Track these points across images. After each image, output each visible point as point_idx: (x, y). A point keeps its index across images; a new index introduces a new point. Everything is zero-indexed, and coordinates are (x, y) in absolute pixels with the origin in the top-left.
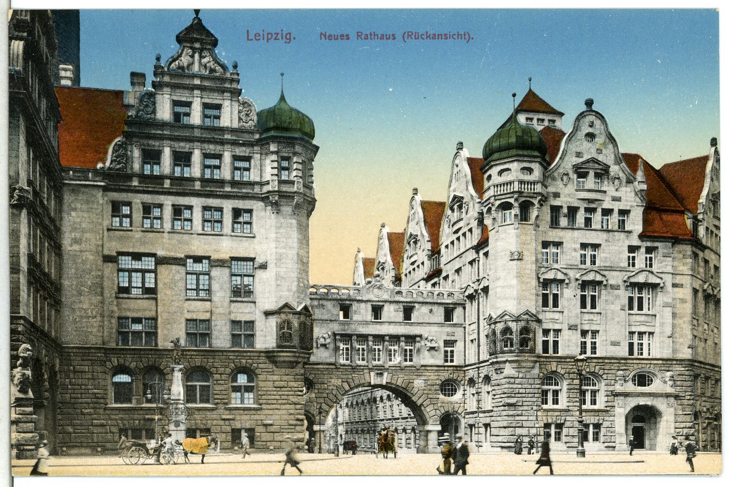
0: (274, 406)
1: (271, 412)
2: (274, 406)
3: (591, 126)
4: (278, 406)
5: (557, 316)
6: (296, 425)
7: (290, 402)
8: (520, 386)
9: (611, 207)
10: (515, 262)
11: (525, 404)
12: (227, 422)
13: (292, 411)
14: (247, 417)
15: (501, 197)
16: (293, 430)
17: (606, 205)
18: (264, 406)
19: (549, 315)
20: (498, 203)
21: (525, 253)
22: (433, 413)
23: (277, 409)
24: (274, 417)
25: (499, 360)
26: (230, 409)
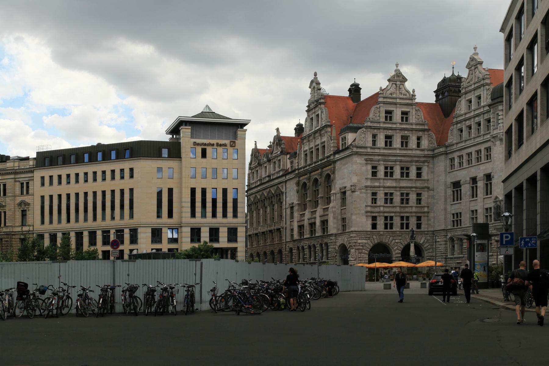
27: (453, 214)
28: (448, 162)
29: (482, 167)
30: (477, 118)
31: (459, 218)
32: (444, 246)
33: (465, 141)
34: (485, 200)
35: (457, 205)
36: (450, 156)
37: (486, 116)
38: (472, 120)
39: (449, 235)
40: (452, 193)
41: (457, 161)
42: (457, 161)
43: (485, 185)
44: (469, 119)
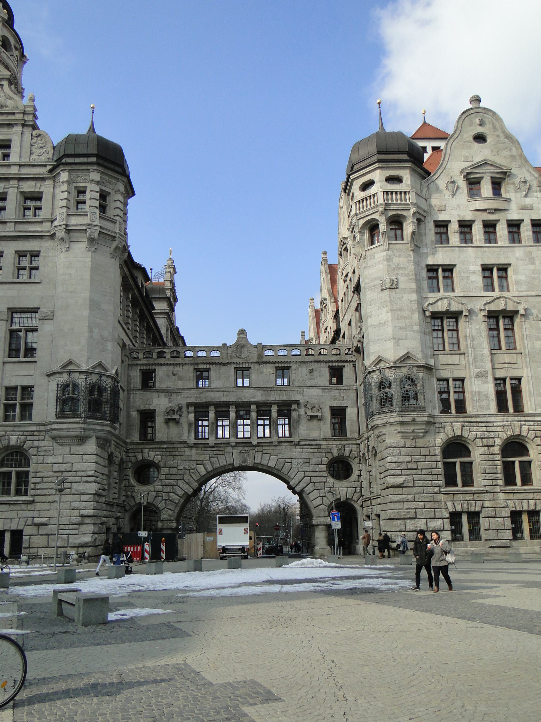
2: (51, 498)
3: (481, 125)
5: (455, 359)
7: (73, 492)
8: (408, 459)
9: (521, 218)
10: (387, 292)
11: (417, 484)
13: (76, 505)
14: (14, 514)
15: (362, 215)
16: (76, 531)
17: (514, 216)
18: (37, 499)
20: (362, 222)
21: (401, 280)
22: (318, 501)
24: (50, 513)
25: (376, 422)
34: (8, 367)
37: (28, 187)
43: (8, 333)
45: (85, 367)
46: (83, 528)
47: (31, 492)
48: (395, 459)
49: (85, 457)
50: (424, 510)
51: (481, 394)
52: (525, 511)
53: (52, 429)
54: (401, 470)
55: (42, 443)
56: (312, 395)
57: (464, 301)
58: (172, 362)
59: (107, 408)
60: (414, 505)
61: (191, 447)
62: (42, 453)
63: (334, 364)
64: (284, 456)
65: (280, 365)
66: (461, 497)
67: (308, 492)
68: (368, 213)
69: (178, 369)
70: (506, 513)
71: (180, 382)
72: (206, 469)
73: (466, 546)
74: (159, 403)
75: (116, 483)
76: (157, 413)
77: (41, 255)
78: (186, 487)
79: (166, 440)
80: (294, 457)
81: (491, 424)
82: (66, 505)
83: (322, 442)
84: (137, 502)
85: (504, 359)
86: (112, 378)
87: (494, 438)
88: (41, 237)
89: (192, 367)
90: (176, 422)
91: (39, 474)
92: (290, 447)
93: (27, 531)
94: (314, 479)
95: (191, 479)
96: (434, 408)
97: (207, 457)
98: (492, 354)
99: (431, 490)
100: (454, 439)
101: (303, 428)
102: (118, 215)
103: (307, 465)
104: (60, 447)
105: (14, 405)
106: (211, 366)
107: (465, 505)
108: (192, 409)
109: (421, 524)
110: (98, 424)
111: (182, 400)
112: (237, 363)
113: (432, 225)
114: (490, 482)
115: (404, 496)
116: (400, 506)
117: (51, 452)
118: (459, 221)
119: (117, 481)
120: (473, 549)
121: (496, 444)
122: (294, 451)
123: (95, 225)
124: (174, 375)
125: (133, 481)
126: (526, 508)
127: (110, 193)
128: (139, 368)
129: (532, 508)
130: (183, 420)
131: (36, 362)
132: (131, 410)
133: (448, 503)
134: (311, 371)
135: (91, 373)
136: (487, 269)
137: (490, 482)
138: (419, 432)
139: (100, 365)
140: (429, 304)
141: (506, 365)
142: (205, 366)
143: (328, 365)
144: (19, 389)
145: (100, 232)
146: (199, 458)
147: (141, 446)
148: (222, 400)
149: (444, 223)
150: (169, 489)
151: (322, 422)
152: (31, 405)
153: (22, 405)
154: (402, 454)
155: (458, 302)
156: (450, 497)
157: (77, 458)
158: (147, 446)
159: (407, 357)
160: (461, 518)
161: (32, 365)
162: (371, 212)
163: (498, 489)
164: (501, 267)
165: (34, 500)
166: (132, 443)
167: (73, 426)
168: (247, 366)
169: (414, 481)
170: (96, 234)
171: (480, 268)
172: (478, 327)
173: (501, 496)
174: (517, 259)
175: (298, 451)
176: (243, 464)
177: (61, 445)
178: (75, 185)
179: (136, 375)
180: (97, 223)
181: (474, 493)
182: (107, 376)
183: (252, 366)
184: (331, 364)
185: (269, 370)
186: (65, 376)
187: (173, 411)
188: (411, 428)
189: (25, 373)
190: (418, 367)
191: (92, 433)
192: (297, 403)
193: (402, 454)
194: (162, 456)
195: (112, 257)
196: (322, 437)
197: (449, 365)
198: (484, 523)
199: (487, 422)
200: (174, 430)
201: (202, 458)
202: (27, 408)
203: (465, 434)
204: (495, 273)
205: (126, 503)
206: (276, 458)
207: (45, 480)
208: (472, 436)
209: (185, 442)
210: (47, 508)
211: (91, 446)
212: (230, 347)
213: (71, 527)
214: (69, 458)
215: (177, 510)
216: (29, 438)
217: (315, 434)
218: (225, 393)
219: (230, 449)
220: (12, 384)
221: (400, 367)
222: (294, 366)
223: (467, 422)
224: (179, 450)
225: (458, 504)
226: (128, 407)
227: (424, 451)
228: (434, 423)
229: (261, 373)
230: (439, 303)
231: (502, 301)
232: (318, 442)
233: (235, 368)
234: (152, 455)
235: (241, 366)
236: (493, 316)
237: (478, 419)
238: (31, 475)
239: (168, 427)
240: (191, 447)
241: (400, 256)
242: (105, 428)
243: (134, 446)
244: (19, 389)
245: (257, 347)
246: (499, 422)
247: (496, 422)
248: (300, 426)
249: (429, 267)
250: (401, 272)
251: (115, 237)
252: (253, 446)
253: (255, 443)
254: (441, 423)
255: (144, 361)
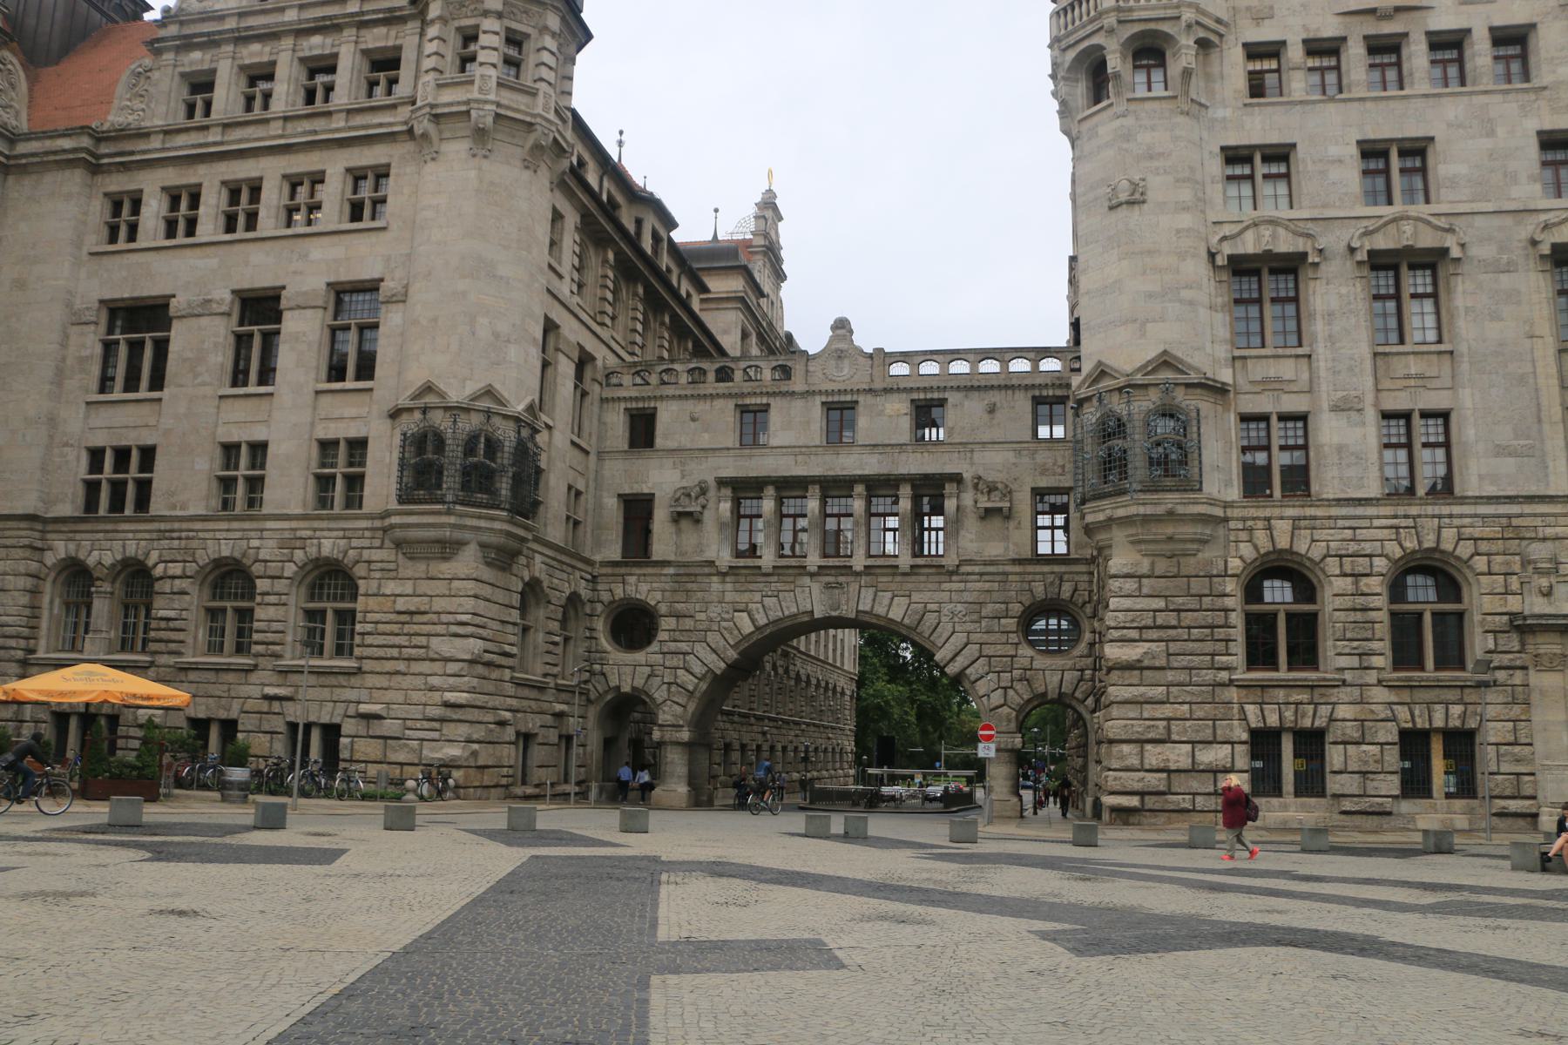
0: (389, 666)
1: (381, 681)
2: (389, 666)
4: (401, 666)
5: (1286, 369)
6: (442, 720)
7: (432, 655)
8: (1161, 604)
12: (276, 706)
13: (435, 681)
14: (325, 693)
16: (435, 735)
18: (368, 665)
19: (1258, 370)
22: (997, 698)
23: (398, 673)
24: (390, 696)
26: (284, 672)
27: (96, 455)
28: (98, 211)
29: (319, 251)
30: (316, 39)
31: (134, 472)
32: (25, 599)
33: (226, 126)
34: (325, 400)
35: (131, 408)
36: (118, 183)
38: (287, 42)
39: (61, 549)
40: (98, 349)
41: (153, 211)
42: (153, 211)
43: (327, 332)
44: (272, 36)
45: (456, 395)
46: (450, 730)
47: (357, 651)
48: (1127, 603)
49: (456, 584)
50: (1188, 723)
51: (1349, 452)
52: (1437, 730)
53: (392, 527)
54: (1140, 628)
55: (376, 555)
56: (992, 463)
57: (1312, 228)
58: (689, 392)
59: (504, 487)
60: (1167, 710)
61: (725, 574)
62: (378, 575)
63: (1045, 393)
64: (926, 596)
65: (922, 396)
66: (1281, 694)
67: (973, 678)
68: (1082, 33)
69: (700, 407)
70: (1389, 733)
71: (706, 436)
72: (753, 621)
73: (1285, 808)
74: (661, 478)
75: (555, 644)
76: (657, 501)
77: (393, 172)
78: (711, 659)
79: (672, 558)
80: (947, 599)
81: (1366, 523)
82: (419, 681)
83: (1009, 568)
84: (612, 684)
85: (1407, 366)
86: (517, 419)
87: (1370, 556)
88: (391, 137)
89: (731, 404)
90: (695, 519)
91: (370, 617)
92: (937, 578)
93: (348, 727)
94: (988, 650)
95: (722, 642)
96: (1228, 483)
97: (757, 597)
98: (1375, 354)
99: (1209, 676)
100: (1272, 557)
101: (969, 536)
102: (541, 79)
103: (975, 617)
104: (410, 563)
105: (333, 477)
106: (772, 401)
107: (1289, 714)
108: (728, 492)
109: (1178, 755)
110: (480, 517)
111: (709, 470)
112: (827, 393)
113: (1237, 54)
114: (1355, 661)
115: (1142, 689)
116: (1132, 712)
117: (391, 573)
118: (1305, 41)
119: (557, 639)
120: (1302, 816)
121: (1375, 569)
122: (946, 586)
123: (486, 102)
124: (693, 419)
125: (605, 643)
126: (1439, 722)
127: (528, 36)
128: (623, 405)
129: (1455, 723)
130: (708, 516)
131: (371, 390)
132: (605, 494)
133: (1247, 707)
134: (992, 410)
135: (467, 410)
136: (1372, 152)
137: (1355, 661)
138: (1184, 541)
139: (489, 392)
140: (1224, 238)
141: (1412, 382)
142: (758, 401)
143: (1030, 394)
144: (342, 447)
145: (498, 116)
146: (738, 597)
147: (623, 570)
148: (794, 473)
149: (1271, 48)
150: (676, 661)
151: (1012, 524)
152: (362, 476)
153: (347, 477)
154: (1145, 591)
155: (1295, 233)
156: (1256, 695)
157: (440, 587)
158: (637, 571)
159: (1166, 361)
160: (1280, 744)
161: (365, 397)
162: (1090, 29)
163: (1372, 677)
164: (1408, 145)
165: (360, 669)
166: (604, 564)
167: (427, 521)
168: (848, 398)
169: (1169, 655)
170: (490, 120)
171: (1354, 151)
172: (1344, 290)
173: (1380, 694)
174: (1450, 125)
175: (955, 586)
176: (834, 614)
177: (411, 559)
178: (457, 24)
179: (617, 425)
180: (492, 97)
181: (1312, 687)
182: (505, 417)
183: (861, 399)
184: (1037, 393)
185: (898, 408)
186: (417, 415)
187: (689, 495)
188: (1169, 530)
189: (353, 412)
190: (1188, 386)
191: (467, 535)
192: (957, 479)
193: (1145, 591)
194: (663, 591)
195: (527, 167)
196: (1012, 555)
197: (1272, 379)
198: (1335, 756)
199: (1359, 517)
200: (690, 538)
201: (746, 597)
202: (355, 482)
203: (1301, 547)
204: (1395, 162)
205: (590, 686)
206: (905, 601)
207: (381, 627)
208: (1316, 553)
209: (711, 563)
210: (385, 684)
211: (468, 562)
212: (815, 357)
213: (426, 725)
214: (425, 586)
215: (692, 707)
216: (355, 543)
217: (994, 550)
218: (800, 458)
219: (807, 580)
220: (331, 436)
221: (1145, 386)
222: (952, 398)
223: (1305, 518)
224: (699, 579)
225: (1273, 711)
226: (598, 487)
227: (1197, 586)
228: (1226, 520)
229: (881, 413)
230: (1249, 236)
231: (1408, 228)
232: (1001, 569)
233: (823, 403)
234: (643, 588)
235: (836, 398)
236: (1381, 262)
237: (1334, 511)
238: (359, 616)
239: (679, 532)
240: (725, 574)
241: (1153, 129)
242: (497, 525)
243: (609, 570)
244: (342, 447)
245: (871, 356)
246: (1386, 517)
247: (1378, 517)
248: (962, 533)
249: (1230, 153)
250: (1156, 164)
251: (531, 124)
252: (858, 574)
253: (858, 567)
254: (1244, 519)
255: (634, 393)
